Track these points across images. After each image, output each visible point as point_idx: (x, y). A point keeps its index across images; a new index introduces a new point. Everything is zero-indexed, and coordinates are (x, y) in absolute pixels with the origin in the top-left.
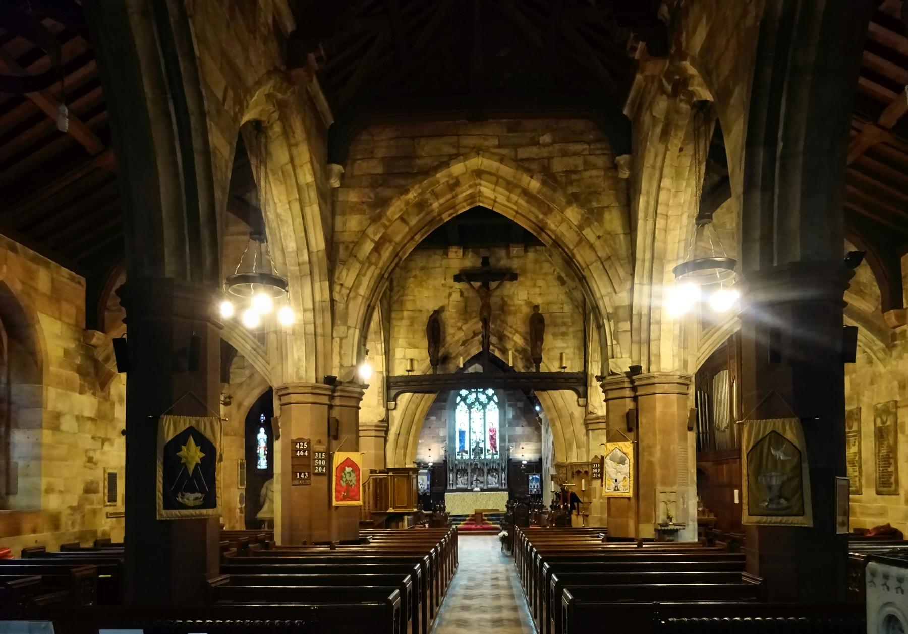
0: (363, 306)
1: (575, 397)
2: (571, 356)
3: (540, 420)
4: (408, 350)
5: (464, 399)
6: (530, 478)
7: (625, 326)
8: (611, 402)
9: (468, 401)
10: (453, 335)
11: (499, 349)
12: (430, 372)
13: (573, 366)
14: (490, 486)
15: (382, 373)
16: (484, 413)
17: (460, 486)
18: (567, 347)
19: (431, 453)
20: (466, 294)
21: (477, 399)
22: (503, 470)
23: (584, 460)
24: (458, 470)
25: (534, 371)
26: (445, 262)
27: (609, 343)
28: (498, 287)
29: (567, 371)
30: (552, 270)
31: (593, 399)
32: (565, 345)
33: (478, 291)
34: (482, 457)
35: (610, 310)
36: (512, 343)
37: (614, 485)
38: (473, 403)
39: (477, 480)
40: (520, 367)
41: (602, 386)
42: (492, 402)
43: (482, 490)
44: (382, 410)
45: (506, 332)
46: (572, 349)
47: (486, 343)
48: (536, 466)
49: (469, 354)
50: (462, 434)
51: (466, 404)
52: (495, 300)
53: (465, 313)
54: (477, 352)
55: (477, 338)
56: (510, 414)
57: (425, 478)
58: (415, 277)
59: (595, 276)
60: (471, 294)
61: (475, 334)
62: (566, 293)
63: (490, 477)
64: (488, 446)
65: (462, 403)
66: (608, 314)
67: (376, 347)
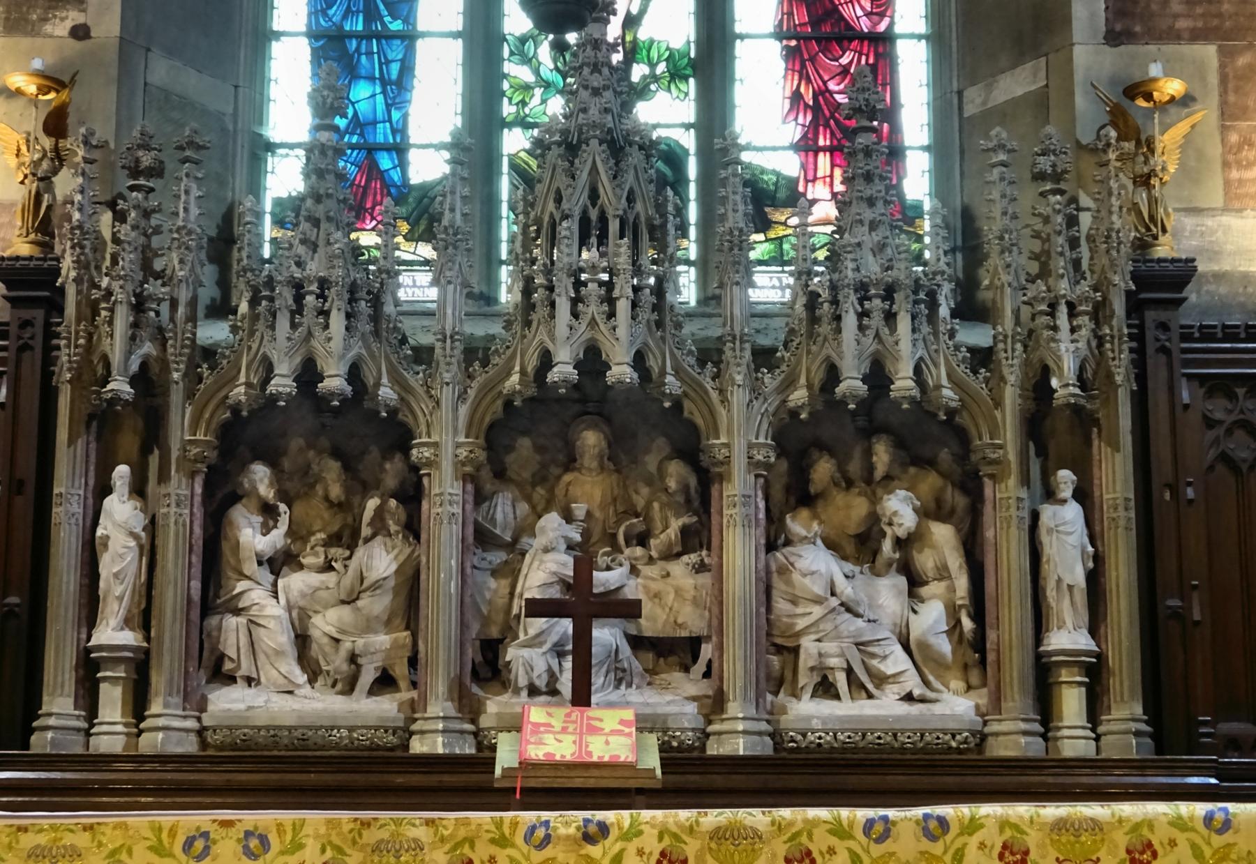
14: (809, 714)
22: (1056, 434)
24: (243, 437)
39: (580, 603)
43: (690, 776)
63: (815, 564)
64: (766, 118)
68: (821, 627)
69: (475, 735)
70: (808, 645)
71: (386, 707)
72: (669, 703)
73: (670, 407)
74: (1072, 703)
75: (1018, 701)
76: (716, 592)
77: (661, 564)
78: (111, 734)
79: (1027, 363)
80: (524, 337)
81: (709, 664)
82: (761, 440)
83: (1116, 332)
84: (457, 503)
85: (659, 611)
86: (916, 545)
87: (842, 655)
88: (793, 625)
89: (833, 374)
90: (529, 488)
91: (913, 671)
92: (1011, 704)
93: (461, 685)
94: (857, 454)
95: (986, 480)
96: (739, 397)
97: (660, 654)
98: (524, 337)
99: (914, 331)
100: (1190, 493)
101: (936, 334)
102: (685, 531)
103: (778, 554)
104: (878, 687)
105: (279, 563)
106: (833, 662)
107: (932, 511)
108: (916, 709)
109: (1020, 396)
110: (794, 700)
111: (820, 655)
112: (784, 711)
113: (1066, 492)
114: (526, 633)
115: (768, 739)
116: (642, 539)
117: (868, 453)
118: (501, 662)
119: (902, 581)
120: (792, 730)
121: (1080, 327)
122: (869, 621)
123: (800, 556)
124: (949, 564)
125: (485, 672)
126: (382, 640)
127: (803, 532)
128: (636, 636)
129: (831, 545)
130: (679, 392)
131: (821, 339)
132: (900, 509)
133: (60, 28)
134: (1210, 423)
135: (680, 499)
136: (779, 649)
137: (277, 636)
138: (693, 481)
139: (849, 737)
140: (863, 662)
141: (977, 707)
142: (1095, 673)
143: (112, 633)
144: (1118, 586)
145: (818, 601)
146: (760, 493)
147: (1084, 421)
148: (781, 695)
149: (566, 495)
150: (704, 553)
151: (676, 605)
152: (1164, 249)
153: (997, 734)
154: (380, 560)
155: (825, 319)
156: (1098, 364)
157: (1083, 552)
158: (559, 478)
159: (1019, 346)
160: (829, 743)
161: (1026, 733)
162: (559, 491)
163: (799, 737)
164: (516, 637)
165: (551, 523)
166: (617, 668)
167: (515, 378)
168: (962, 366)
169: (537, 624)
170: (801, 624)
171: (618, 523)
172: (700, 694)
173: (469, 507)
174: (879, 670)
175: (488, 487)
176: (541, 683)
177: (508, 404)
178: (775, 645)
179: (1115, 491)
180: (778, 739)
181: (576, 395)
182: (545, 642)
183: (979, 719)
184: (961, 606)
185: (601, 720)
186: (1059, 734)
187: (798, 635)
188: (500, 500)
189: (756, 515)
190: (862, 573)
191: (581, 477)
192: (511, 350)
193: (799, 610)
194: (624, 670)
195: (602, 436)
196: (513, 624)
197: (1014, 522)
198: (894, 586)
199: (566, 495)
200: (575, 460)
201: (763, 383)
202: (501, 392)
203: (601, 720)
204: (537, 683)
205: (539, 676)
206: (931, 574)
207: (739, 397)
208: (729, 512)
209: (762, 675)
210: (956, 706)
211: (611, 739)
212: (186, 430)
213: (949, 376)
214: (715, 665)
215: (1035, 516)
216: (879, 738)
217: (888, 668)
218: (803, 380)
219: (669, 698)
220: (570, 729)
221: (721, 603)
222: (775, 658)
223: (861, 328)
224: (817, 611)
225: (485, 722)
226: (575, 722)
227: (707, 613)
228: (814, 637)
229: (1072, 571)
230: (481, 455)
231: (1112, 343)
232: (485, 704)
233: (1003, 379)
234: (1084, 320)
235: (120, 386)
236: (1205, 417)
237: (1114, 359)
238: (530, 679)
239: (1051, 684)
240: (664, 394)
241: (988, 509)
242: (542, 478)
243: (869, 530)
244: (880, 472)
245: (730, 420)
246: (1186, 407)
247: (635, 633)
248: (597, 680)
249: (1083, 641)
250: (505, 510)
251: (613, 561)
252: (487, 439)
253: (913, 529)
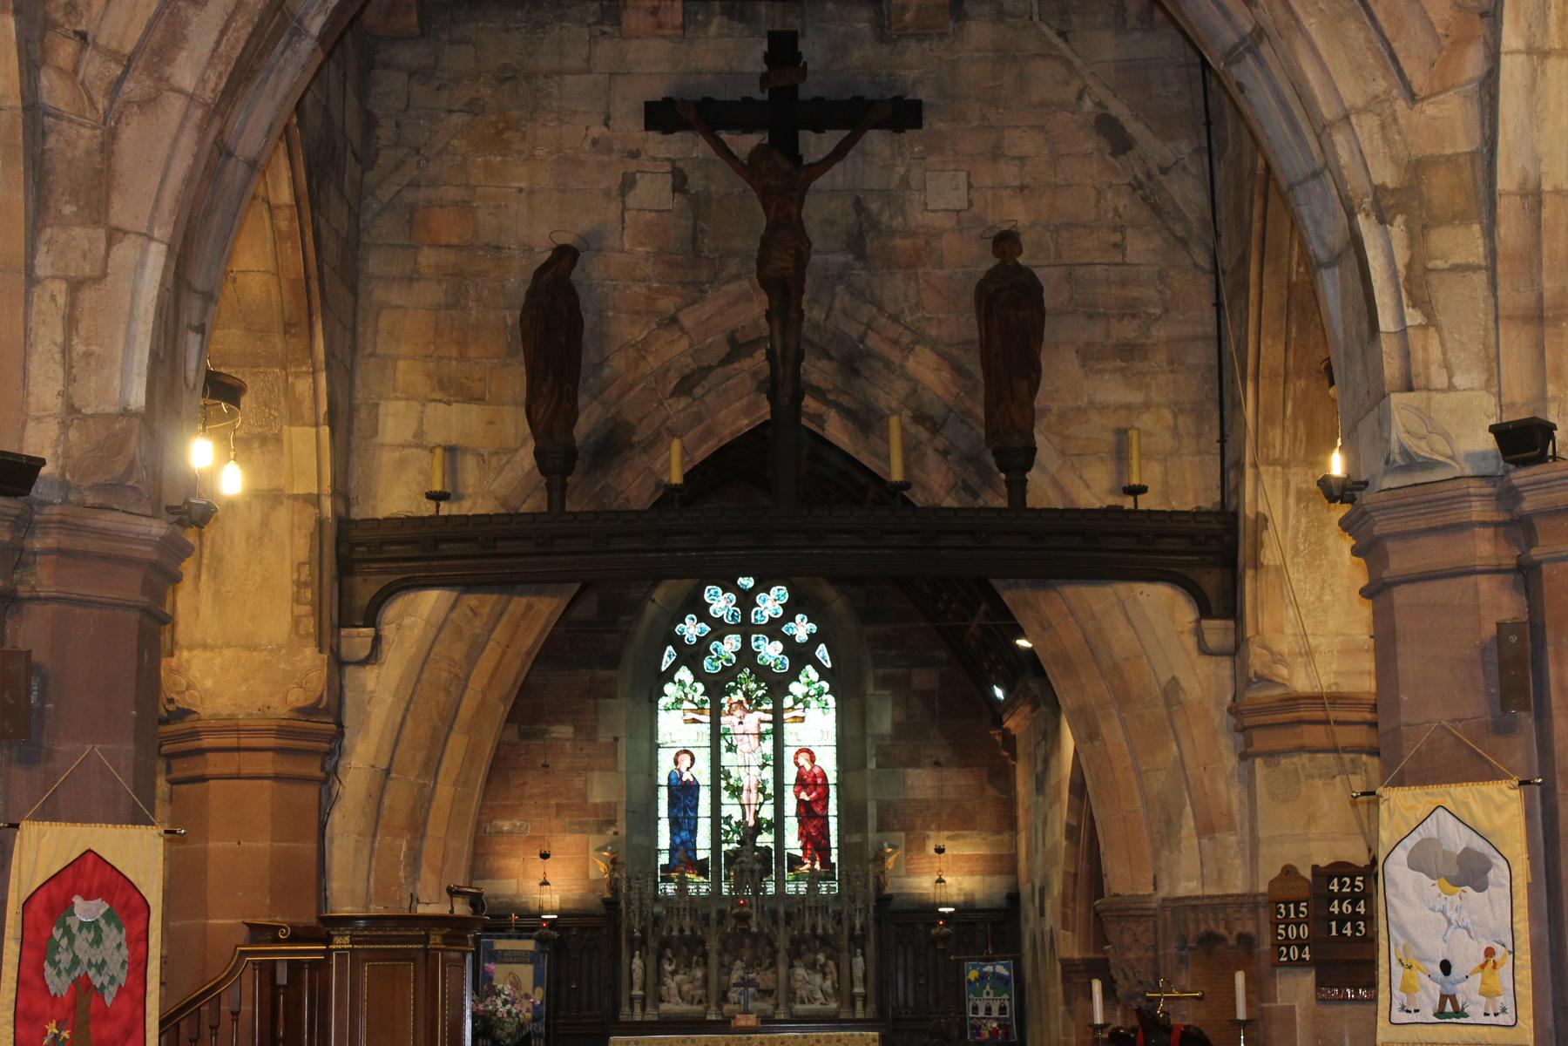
0: (188, 141)
1: (1186, 613)
2: (1165, 441)
3: (1010, 741)
4: (436, 411)
5: (692, 656)
6: (973, 975)
7: (1460, 244)
8: (1401, 595)
9: (707, 665)
10: (642, 349)
11: (847, 413)
12: (535, 503)
13: (1176, 483)
14: (799, 1008)
15: (314, 500)
16: (778, 713)
17: (674, 1007)
18: (1147, 405)
19: (552, 877)
20: (696, 183)
21: (747, 655)
22: (857, 941)
23: (1237, 884)
24: (665, 944)
25: (1002, 503)
26: (605, 49)
27: (1386, 322)
28: (839, 154)
29: (1146, 502)
30: (1071, 92)
31: (1266, 622)
32: (1137, 397)
33: (750, 169)
34: (771, 889)
35: (1385, 174)
36: (901, 387)
37: (1435, 991)
38: (729, 673)
39: (745, 983)
40: (937, 487)
41: (1346, 525)
42: (810, 672)
44: (311, 660)
45: (873, 341)
46: (1167, 414)
47: (784, 386)
48: (994, 926)
49: (710, 432)
50: (684, 793)
51: (699, 675)
52: (822, 208)
53: (690, 263)
54: (745, 424)
55: (746, 363)
56: (884, 719)
57: (526, 972)
58: (474, 108)
59: (1311, 24)
60: (723, 182)
61: (737, 348)
62: (1136, 186)
63: (800, 972)
64: (793, 843)
65: (684, 674)
66: (1379, 191)
67: (288, 390)
71: (700, 1008)
74: (859, 1005)
78: (638, 1018)
105: (674, 973)
107: (828, 958)
126: (700, 992)
132: (821, 958)
133: (610, 832)
137: (674, 991)
142: (865, 998)
143: (637, 992)
147: (864, 937)
152: (888, 891)
154: (699, 973)
165: (738, 963)
210: (833, 1005)
212: (652, 943)
235: (637, 934)
250: (727, 959)
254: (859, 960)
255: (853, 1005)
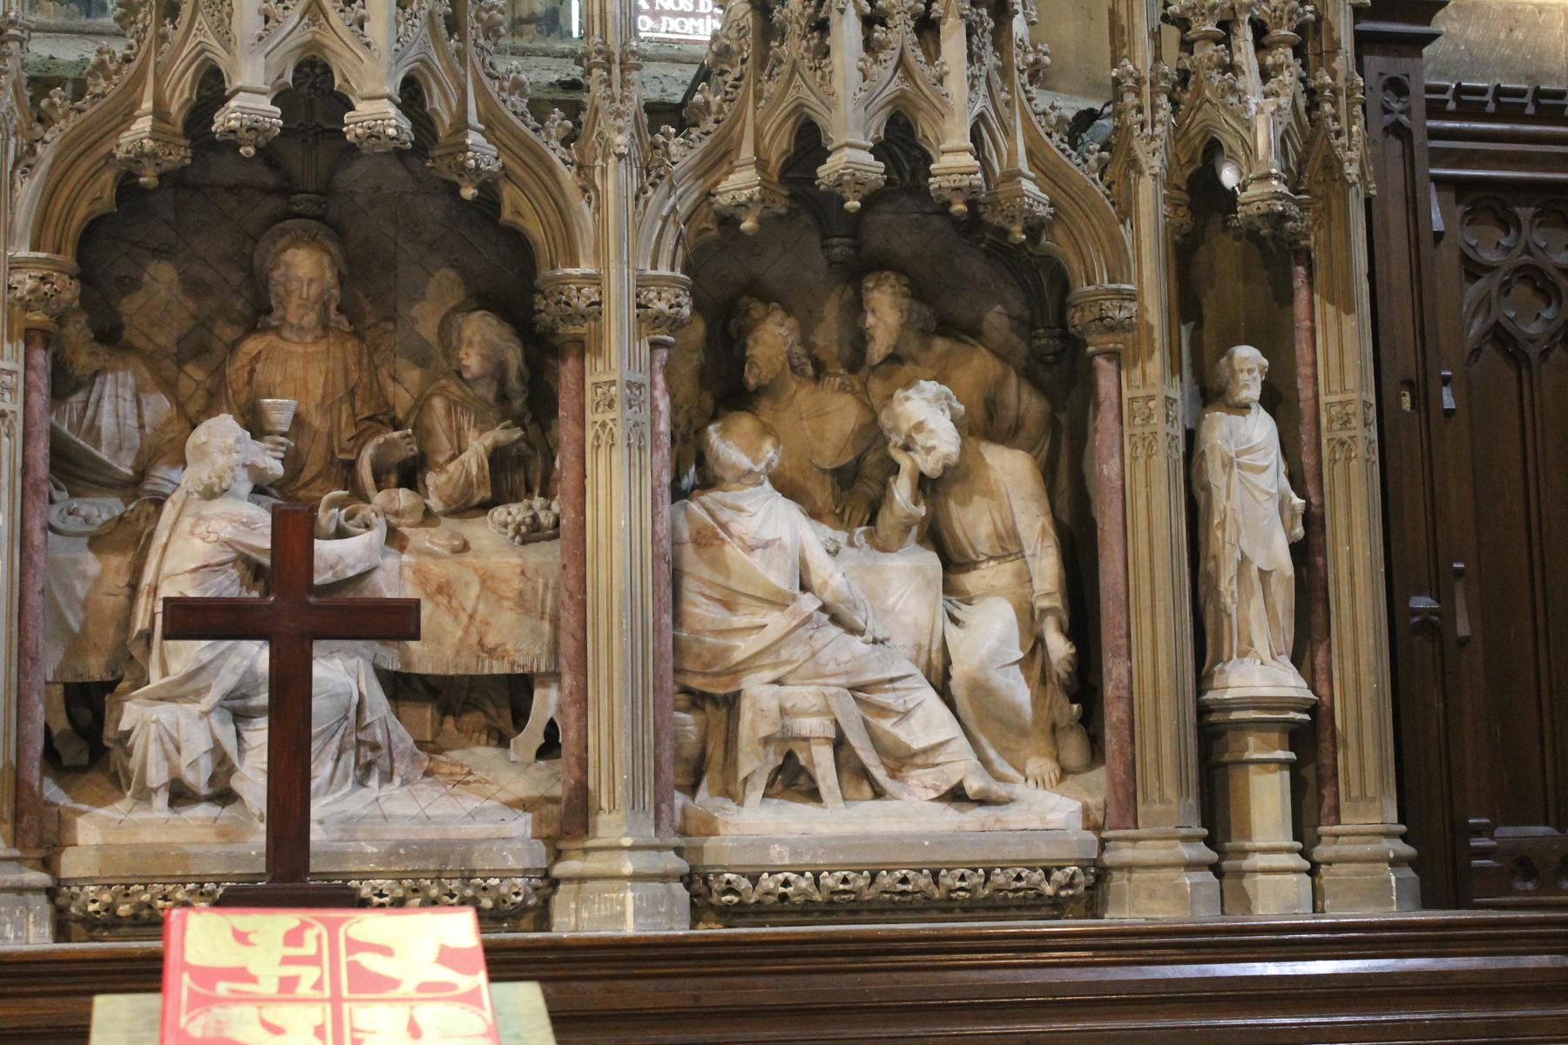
14: (761, 833)
22: (1236, 276)
39: (285, 606)
63: (768, 527)
68: (785, 654)
69: (51, 893)
70: (757, 691)
72: (472, 815)
73: (477, 200)
74: (1267, 799)
75: (1169, 798)
76: (572, 584)
77: (449, 524)
79: (1179, 134)
80: (163, 38)
81: (551, 729)
82: (664, 270)
83: (1341, 82)
84: (12, 390)
85: (447, 620)
86: (956, 489)
87: (826, 711)
88: (728, 650)
89: (809, 142)
90: (169, 367)
91: (963, 740)
92: (1158, 807)
93: (19, 784)
94: (831, 310)
95: (1101, 361)
96: (616, 181)
97: (445, 710)
98: (163, 38)
99: (971, 57)
100: (1448, 401)
101: (1005, 72)
102: (498, 458)
103: (694, 506)
104: (894, 773)
106: (810, 725)
107: (985, 423)
108: (974, 817)
109: (1166, 199)
110: (730, 805)
111: (783, 712)
112: (709, 827)
113: (1251, 391)
114: (165, 673)
115: (678, 887)
116: (410, 474)
117: (857, 307)
118: (109, 733)
119: (930, 561)
120: (729, 869)
121: (1278, 68)
122: (875, 641)
123: (740, 510)
124: (1022, 528)
125: (73, 753)
127: (745, 462)
128: (396, 673)
129: (788, 487)
130: (495, 167)
131: (785, 68)
132: (927, 416)
134: (1473, 269)
135: (487, 391)
136: (696, 700)
138: (514, 357)
139: (845, 881)
140: (866, 723)
141: (1086, 811)
144: (1352, 573)
145: (778, 602)
146: (660, 379)
147: (1277, 253)
148: (703, 793)
149: (249, 383)
150: (538, 502)
151: (482, 608)
153: (1130, 867)
155: (794, 29)
156: (1309, 143)
157: (1283, 504)
158: (233, 347)
159: (1163, 100)
160: (803, 892)
161: (1191, 866)
162: (236, 370)
163: (744, 884)
164: (142, 680)
165: (221, 434)
166: (359, 743)
167: (143, 125)
168: (1056, 137)
169: (189, 654)
170: (743, 648)
171: (360, 440)
172: (535, 793)
173: (40, 400)
174: (897, 741)
175: (82, 362)
176: (198, 779)
177: (127, 187)
178: (686, 690)
179: (1344, 390)
180: (699, 885)
181: (271, 180)
182: (208, 688)
183: (1091, 836)
184: (1044, 612)
185: (386, 951)
186: (1247, 864)
187: (736, 671)
188: (108, 389)
189: (653, 425)
190: (851, 544)
191: (282, 344)
192: (134, 65)
193: (740, 620)
194: (375, 747)
195: (326, 260)
196: (136, 652)
197: (1161, 445)
198: (918, 570)
199: (249, 383)
200: (269, 311)
201: (667, 154)
202: (111, 155)
203: (386, 951)
204: (190, 777)
205: (193, 764)
206: (984, 547)
207: (616, 181)
208: (599, 418)
209: (667, 755)
210: (1047, 811)
211: (427, 1014)
213: (1030, 154)
214: (568, 737)
215: (1191, 437)
216: (904, 880)
217: (915, 735)
218: (747, 152)
219: (472, 803)
220: (304, 989)
221: (582, 605)
222: (688, 718)
223: (870, 46)
224: (776, 622)
225: (72, 864)
226: (314, 960)
227: (546, 627)
228: (769, 675)
229: (1268, 543)
230: (69, 290)
231: (1335, 104)
232: (71, 826)
233: (1133, 163)
234: (1284, 54)
236: (1465, 258)
237: (1338, 134)
238: (173, 769)
239: (1225, 765)
240: (463, 168)
241: (1105, 422)
242: (194, 347)
243: (859, 460)
244: (879, 348)
245: (601, 226)
246: (1438, 236)
247: (394, 665)
248: (321, 771)
249: (1288, 683)
250: (118, 410)
251: (349, 517)
252: (80, 255)
253: (955, 458)
254: (1248, 437)
255: (1217, 814)
